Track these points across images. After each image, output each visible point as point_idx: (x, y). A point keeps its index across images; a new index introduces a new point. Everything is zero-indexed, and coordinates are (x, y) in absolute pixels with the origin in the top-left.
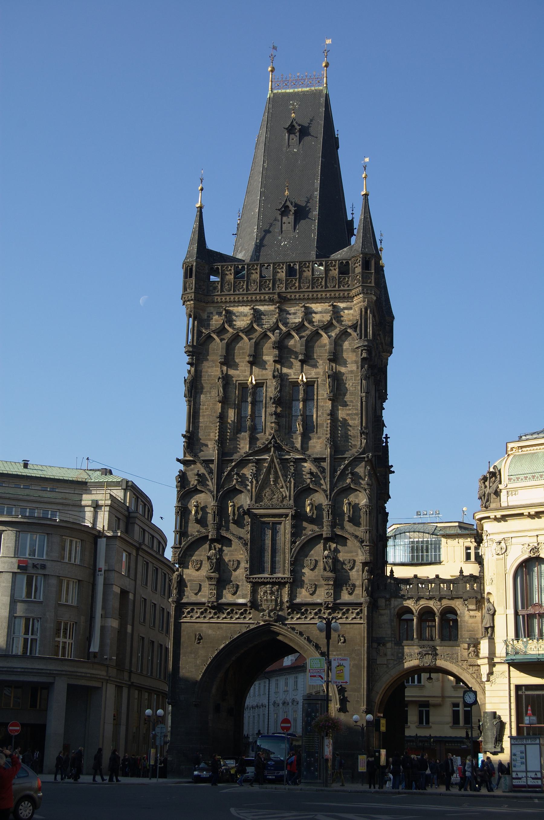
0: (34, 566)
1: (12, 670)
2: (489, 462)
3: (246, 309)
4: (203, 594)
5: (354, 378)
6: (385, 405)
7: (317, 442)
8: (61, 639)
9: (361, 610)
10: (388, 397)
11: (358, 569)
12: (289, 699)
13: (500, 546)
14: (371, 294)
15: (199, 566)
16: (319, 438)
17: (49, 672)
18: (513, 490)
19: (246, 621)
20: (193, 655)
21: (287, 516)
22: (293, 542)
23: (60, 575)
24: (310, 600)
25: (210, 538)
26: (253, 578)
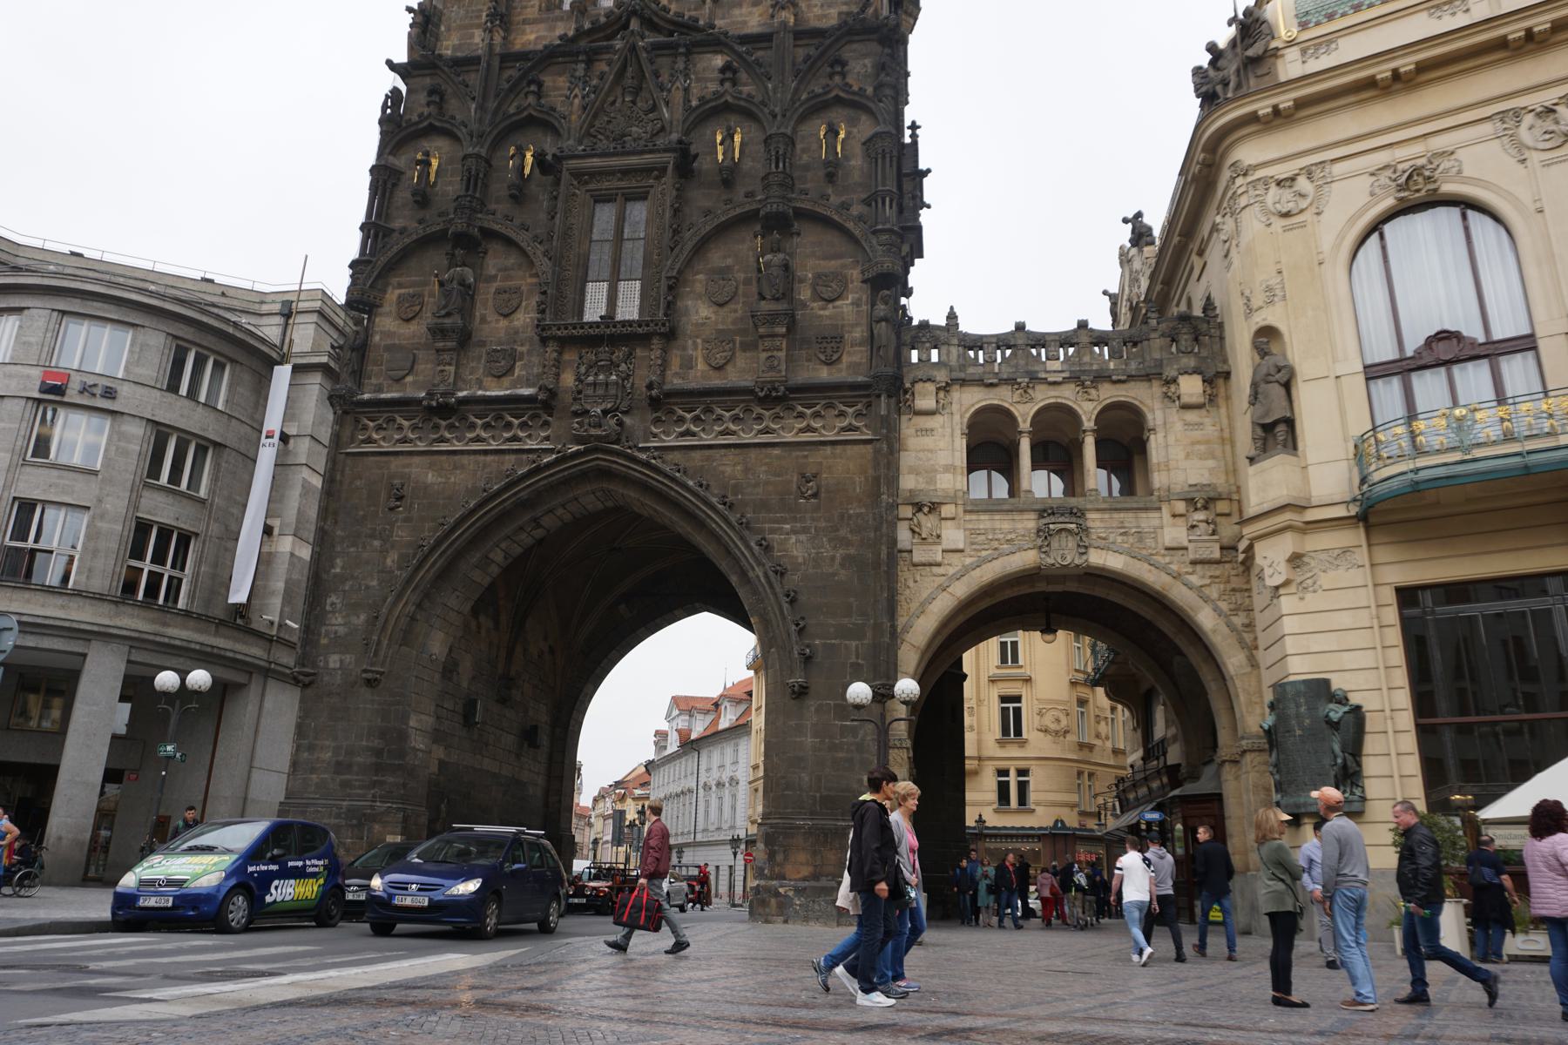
4: (421, 378)
7: (750, 13)
8: (147, 566)
9: (869, 405)
11: (860, 299)
12: (725, 779)
15: (418, 308)
17: (67, 624)
18: (1320, 44)
19: (531, 444)
20: (377, 543)
21: (663, 170)
22: (676, 232)
23: (156, 419)
24: (716, 382)
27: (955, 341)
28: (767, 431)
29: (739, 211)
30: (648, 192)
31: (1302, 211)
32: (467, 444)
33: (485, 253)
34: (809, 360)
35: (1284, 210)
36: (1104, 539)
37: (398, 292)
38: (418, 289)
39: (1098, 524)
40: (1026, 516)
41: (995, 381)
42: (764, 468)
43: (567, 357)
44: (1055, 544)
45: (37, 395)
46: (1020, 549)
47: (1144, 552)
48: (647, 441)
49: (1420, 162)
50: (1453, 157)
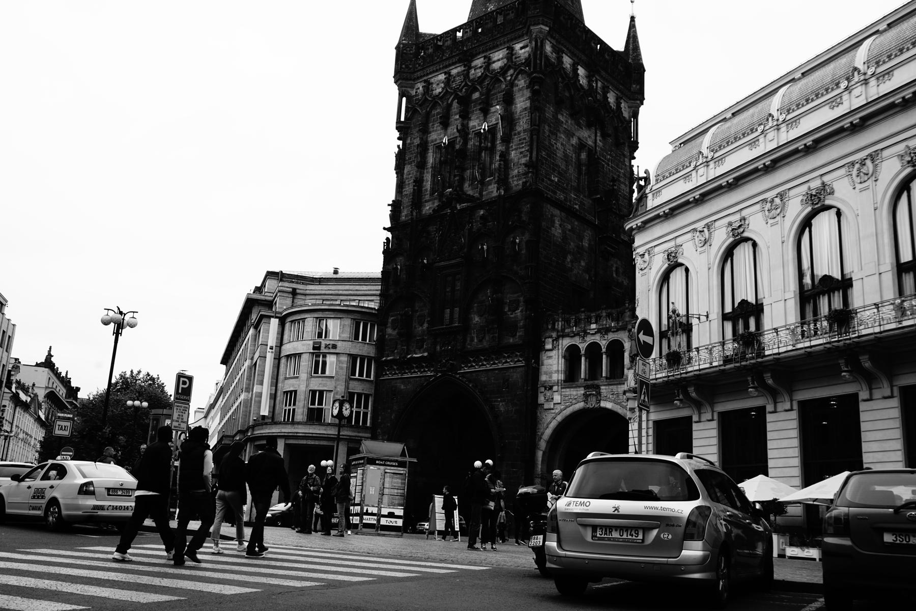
0: (327, 346)
1: (295, 434)
2: (638, 167)
3: (442, 77)
5: (527, 114)
6: (636, 154)
10: (639, 145)
11: (523, 309)
13: (643, 259)
14: (539, 24)
15: (396, 325)
17: (326, 436)
20: (389, 411)
23: (351, 353)
27: (560, 320)
28: (494, 364)
31: (645, 268)
36: (606, 396)
37: (392, 318)
39: (604, 391)
40: (581, 389)
41: (573, 335)
42: (493, 378)
43: (439, 340)
44: (589, 400)
45: (312, 351)
46: (578, 402)
47: (619, 401)
49: (673, 249)
50: (682, 247)
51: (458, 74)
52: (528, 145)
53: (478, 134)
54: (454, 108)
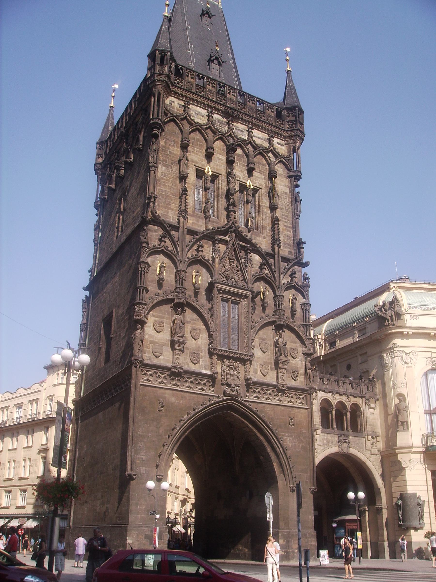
3: (204, 112)
4: (166, 358)
5: (287, 198)
11: (302, 359)
16: (264, 238)
19: (209, 392)
20: (155, 423)
21: (246, 297)
24: (263, 380)
25: (176, 301)
26: (219, 350)
29: (270, 320)
30: (239, 303)
32: (184, 389)
33: (185, 311)
34: (289, 378)
35: (408, 362)
38: (161, 320)
48: (246, 398)
51: (219, 121)
52: (291, 224)
53: (243, 187)
54: (217, 147)
